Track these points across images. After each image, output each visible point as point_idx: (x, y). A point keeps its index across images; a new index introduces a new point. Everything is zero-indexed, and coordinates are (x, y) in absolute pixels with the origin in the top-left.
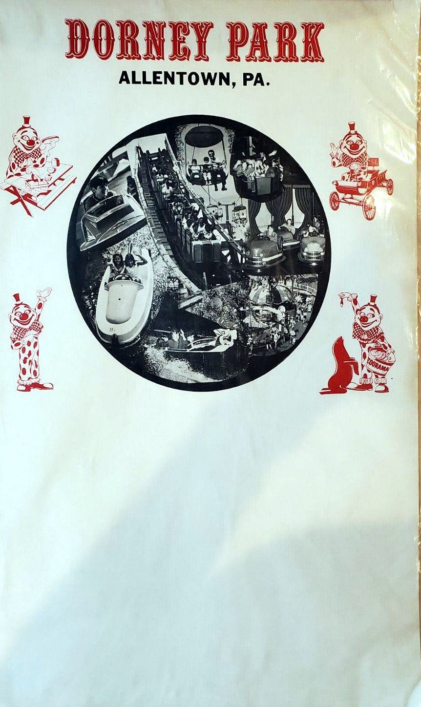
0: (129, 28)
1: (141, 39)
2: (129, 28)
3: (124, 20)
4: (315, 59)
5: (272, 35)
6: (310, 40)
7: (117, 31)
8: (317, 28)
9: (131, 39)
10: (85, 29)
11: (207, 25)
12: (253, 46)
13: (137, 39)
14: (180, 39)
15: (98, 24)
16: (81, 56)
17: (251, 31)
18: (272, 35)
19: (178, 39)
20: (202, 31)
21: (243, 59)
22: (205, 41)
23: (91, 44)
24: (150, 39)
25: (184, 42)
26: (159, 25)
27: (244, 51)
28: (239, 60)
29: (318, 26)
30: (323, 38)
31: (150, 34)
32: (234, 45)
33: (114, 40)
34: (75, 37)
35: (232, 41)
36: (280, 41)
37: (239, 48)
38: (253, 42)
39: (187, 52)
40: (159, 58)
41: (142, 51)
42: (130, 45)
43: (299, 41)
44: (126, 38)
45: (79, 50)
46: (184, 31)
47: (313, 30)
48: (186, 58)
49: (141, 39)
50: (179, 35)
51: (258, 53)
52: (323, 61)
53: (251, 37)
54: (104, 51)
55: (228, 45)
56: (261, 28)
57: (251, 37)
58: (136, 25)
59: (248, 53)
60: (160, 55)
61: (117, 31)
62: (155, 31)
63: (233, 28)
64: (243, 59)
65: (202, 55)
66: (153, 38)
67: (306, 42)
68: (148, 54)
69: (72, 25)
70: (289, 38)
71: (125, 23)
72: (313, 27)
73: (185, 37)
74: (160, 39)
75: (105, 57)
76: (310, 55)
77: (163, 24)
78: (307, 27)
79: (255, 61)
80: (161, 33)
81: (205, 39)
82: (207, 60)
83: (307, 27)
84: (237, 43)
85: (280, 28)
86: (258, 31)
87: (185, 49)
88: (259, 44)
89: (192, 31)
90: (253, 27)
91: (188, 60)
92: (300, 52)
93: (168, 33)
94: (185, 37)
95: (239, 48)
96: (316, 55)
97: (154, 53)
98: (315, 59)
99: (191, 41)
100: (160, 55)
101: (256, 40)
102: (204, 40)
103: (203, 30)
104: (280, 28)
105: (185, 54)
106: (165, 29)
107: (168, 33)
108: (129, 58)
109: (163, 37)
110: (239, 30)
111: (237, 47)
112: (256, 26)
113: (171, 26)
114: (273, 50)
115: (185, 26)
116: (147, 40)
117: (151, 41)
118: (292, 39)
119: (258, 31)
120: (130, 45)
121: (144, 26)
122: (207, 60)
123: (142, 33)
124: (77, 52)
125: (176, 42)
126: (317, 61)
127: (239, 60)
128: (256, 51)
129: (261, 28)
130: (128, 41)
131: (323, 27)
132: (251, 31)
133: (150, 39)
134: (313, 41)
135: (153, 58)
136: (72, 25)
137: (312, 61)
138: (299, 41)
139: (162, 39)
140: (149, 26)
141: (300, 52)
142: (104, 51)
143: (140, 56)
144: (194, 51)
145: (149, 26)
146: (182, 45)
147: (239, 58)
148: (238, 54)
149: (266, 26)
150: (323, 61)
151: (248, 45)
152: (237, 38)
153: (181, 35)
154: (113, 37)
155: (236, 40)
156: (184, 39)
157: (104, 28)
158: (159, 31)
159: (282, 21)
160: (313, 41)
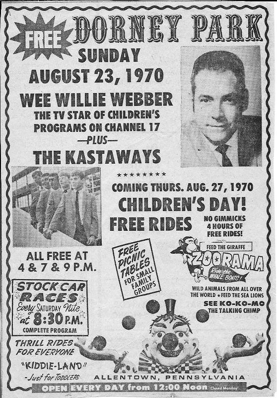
5: (224, 23)
7: (109, 24)
8: (257, 18)
10: (87, 22)
14: (156, 27)
17: (210, 21)
18: (224, 23)
19: (154, 27)
21: (204, 40)
22: (176, 28)
23: (91, 32)
27: (204, 35)
28: (201, 41)
29: (257, 16)
34: (80, 29)
35: (195, 28)
36: (230, 27)
37: (200, 32)
40: (140, 41)
41: (128, 36)
42: (118, 32)
44: (116, 28)
46: (159, 21)
50: (155, 24)
51: (215, 36)
53: (209, 25)
54: (99, 37)
55: (193, 31)
56: (217, 19)
57: (209, 25)
61: (109, 24)
64: (204, 40)
68: (132, 37)
72: (253, 18)
79: (213, 41)
80: (142, 24)
82: (177, 41)
86: (214, 20)
87: (160, 34)
88: (215, 29)
92: (245, 34)
93: (147, 23)
95: (200, 32)
97: (137, 37)
99: (165, 28)
100: (141, 39)
101: (213, 27)
103: (173, 21)
107: (147, 23)
109: (143, 25)
114: (225, 33)
116: (132, 28)
117: (134, 29)
119: (214, 20)
120: (118, 32)
122: (177, 41)
124: (81, 38)
126: (257, 40)
127: (201, 41)
128: (213, 34)
130: (117, 30)
132: (210, 21)
134: (254, 27)
135: (136, 42)
141: (245, 34)
142: (99, 37)
144: (167, 34)
146: (157, 31)
147: (201, 39)
151: (208, 30)
153: (157, 24)
154: (106, 27)
155: (198, 27)
156: (159, 26)
157: (99, 21)
160: (254, 27)
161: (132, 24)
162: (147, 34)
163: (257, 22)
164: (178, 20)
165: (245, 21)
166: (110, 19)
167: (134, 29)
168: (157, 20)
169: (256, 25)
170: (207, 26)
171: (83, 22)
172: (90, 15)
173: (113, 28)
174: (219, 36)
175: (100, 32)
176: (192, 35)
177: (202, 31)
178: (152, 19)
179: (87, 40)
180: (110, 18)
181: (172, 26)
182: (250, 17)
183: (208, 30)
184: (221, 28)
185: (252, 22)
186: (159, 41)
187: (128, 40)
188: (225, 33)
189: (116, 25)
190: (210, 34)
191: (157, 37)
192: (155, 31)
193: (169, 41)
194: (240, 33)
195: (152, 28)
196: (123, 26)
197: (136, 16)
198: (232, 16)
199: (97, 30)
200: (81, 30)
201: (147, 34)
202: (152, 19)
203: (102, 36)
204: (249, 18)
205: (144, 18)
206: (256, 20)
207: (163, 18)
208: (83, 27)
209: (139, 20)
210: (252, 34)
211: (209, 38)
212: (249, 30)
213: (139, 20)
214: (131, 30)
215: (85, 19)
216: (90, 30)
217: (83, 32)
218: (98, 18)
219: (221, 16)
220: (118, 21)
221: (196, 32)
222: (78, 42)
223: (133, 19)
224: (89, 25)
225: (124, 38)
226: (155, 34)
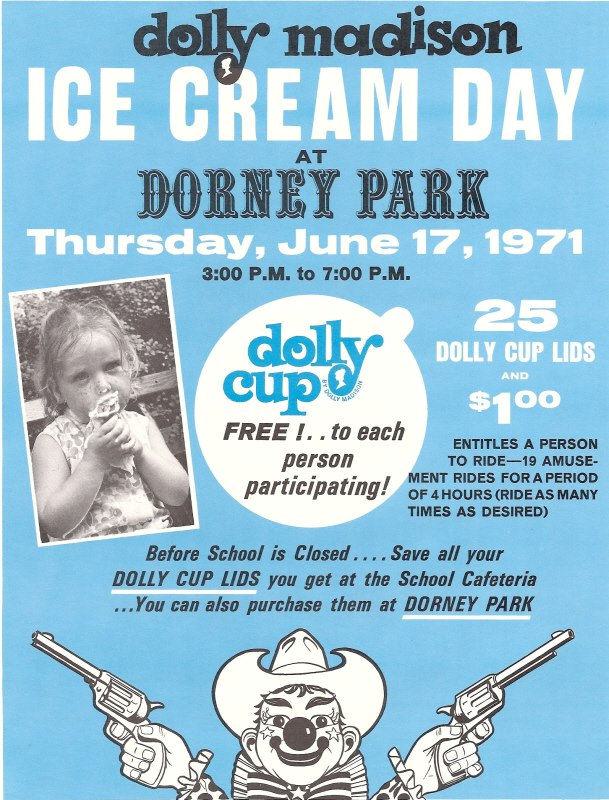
0: (222, 179)
1: (239, 191)
2: (222, 179)
3: (216, 168)
5: (418, 186)
7: (205, 184)
10: (163, 181)
11: (331, 174)
12: (394, 198)
14: (292, 190)
16: (159, 215)
17: (391, 181)
18: (418, 186)
23: (172, 198)
25: (297, 194)
26: (263, 173)
27: (381, 205)
28: (374, 216)
29: (479, 174)
30: (485, 189)
32: (368, 199)
35: (365, 194)
36: (429, 192)
38: (394, 193)
39: (301, 207)
41: (240, 205)
42: (222, 199)
43: (455, 192)
45: (156, 208)
47: (473, 179)
49: (239, 191)
51: (401, 208)
52: (487, 217)
54: (187, 207)
55: (360, 198)
56: (404, 177)
59: (387, 209)
63: (366, 177)
66: (254, 188)
67: (465, 194)
68: (247, 210)
69: (147, 177)
70: (441, 188)
72: (473, 175)
74: (264, 192)
78: (465, 175)
79: (397, 217)
83: (465, 175)
85: (429, 177)
87: (298, 204)
88: (401, 196)
89: (310, 182)
92: (456, 205)
93: (275, 184)
96: (478, 210)
97: (256, 209)
99: (308, 194)
104: (429, 177)
105: (299, 210)
107: (275, 184)
109: (268, 188)
110: (375, 179)
111: (372, 200)
112: (397, 174)
114: (420, 203)
115: (296, 173)
116: (247, 189)
120: (222, 199)
123: (240, 185)
125: (286, 195)
126: (479, 217)
127: (374, 216)
129: (404, 177)
130: (219, 196)
132: (391, 181)
136: (147, 177)
137: (473, 217)
138: (455, 192)
140: (250, 176)
141: (456, 205)
142: (187, 207)
143: (237, 214)
145: (250, 176)
146: (294, 198)
149: (411, 175)
150: (487, 217)
151: (388, 197)
153: (294, 186)
156: (297, 190)
157: (187, 180)
158: (263, 183)
159: (432, 167)
161: (247, 184)
162: (275, 202)
163: (479, 185)
164: (333, 180)
166: (207, 175)
169: (478, 188)
173: (212, 192)
174: (407, 209)
176: (360, 208)
177: (377, 199)
183: (388, 197)
188: (420, 203)
190: (392, 202)
192: (291, 199)
194: (446, 202)
195: (284, 193)
200: (153, 195)
203: (192, 205)
204: (465, 176)
207: (306, 176)
208: (156, 187)
211: (390, 211)
212: (464, 200)
216: (169, 194)
222: (146, 216)
224: (168, 184)
226: (290, 201)
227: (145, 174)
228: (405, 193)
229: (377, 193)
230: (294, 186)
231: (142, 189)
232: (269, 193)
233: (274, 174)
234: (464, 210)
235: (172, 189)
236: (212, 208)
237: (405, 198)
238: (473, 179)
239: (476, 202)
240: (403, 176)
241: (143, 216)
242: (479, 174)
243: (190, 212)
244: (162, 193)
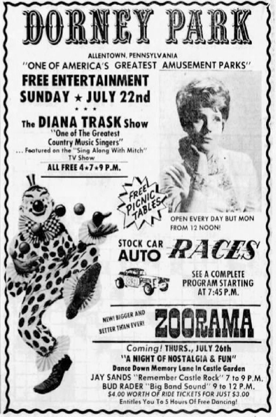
4: (243, 41)
5: (206, 21)
6: (239, 25)
7: (66, 20)
9: (79, 26)
12: (190, 29)
13: (84, 25)
14: (122, 24)
15: (49, 13)
16: (36, 42)
18: (206, 21)
20: (143, 16)
21: (180, 42)
22: (146, 27)
23: (44, 30)
24: (96, 25)
25: (125, 27)
27: (181, 35)
28: (176, 43)
31: (96, 21)
33: (63, 27)
37: (177, 32)
38: (190, 26)
40: (103, 42)
41: (89, 35)
42: (77, 31)
43: (229, 25)
46: (125, 17)
47: (241, 16)
48: (128, 41)
50: (121, 20)
51: (194, 37)
52: (250, 43)
54: (54, 37)
56: (197, 15)
58: (84, 15)
60: (105, 40)
61: (66, 20)
62: (100, 17)
65: (143, 38)
67: (236, 26)
68: (94, 38)
70: (221, 22)
71: (73, 12)
72: (241, 13)
73: (127, 22)
74: (104, 25)
75: (55, 43)
76: (239, 37)
77: (107, 12)
79: (192, 43)
80: (106, 19)
81: (146, 23)
82: (148, 42)
84: (175, 27)
87: (127, 34)
88: (195, 28)
89: (134, 17)
90: (190, 13)
91: (130, 42)
92: (230, 35)
93: (112, 20)
94: (127, 22)
95: (177, 32)
96: (244, 38)
97: (100, 37)
98: (243, 41)
99: (133, 27)
100: (105, 40)
101: (192, 25)
102: (145, 25)
103: (143, 18)
105: (127, 38)
106: (109, 16)
107: (112, 20)
108: (77, 43)
109: (107, 22)
113: (114, 13)
114: (207, 34)
115: (126, 13)
116: (94, 25)
117: (97, 27)
118: (223, 24)
119: (194, 17)
121: (91, 13)
122: (148, 42)
126: (245, 43)
128: (193, 35)
130: (75, 28)
131: (250, 13)
133: (96, 25)
135: (99, 43)
137: (241, 43)
139: (106, 24)
141: (230, 35)
142: (54, 37)
143: (87, 41)
144: (136, 34)
146: (124, 30)
148: (176, 37)
150: (250, 43)
151: (186, 28)
152: (175, 23)
153: (124, 20)
154: (62, 23)
156: (126, 24)
157: (54, 17)
162: (112, 33)
164: (149, 16)
165: (231, 19)
166: (67, 14)
167: (97, 27)
168: (123, 16)
170: (184, 23)
171: (35, 17)
172: (44, 11)
173: (71, 25)
175: (54, 30)
178: (118, 14)
179: (38, 42)
180: (68, 12)
181: (142, 23)
182: (236, 14)
183: (186, 28)
184: (201, 27)
185: (239, 20)
186: (126, 42)
187: (89, 41)
188: (207, 34)
189: (75, 21)
191: (124, 37)
193: (139, 43)
194: (224, 31)
196: (83, 23)
197: (99, 10)
198: (215, 12)
199: (52, 27)
200: (32, 28)
201: (112, 33)
202: (118, 14)
204: (236, 14)
205: (108, 13)
206: (243, 17)
208: (35, 22)
209: (102, 16)
210: (239, 34)
211: (187, 38)
213: (102, 16)
214: (92, 28)
215: (38, 16)
216: (43, 27)
217: (35, 30)
218: (53, 12)
219: (201, 11)
220: (77, 16)
221: (171, 32)
223: (95, 14)
225: (84, 37)
227: (27, 13)
228: (197, 26)
229: (178, 26)
230: (124, 20)
231: (25, 24)
232: (108, 26)
233: (111, 12)
234: (236, 37)
235: (45, 24)
236: (71, 37)
237: (197, 30)
238: (241, 16)
239: (243, 33)
240: (195, 14)
241: (26, 43)
242: (245, 13)
243: (57, 39)
244: (38, 27)
